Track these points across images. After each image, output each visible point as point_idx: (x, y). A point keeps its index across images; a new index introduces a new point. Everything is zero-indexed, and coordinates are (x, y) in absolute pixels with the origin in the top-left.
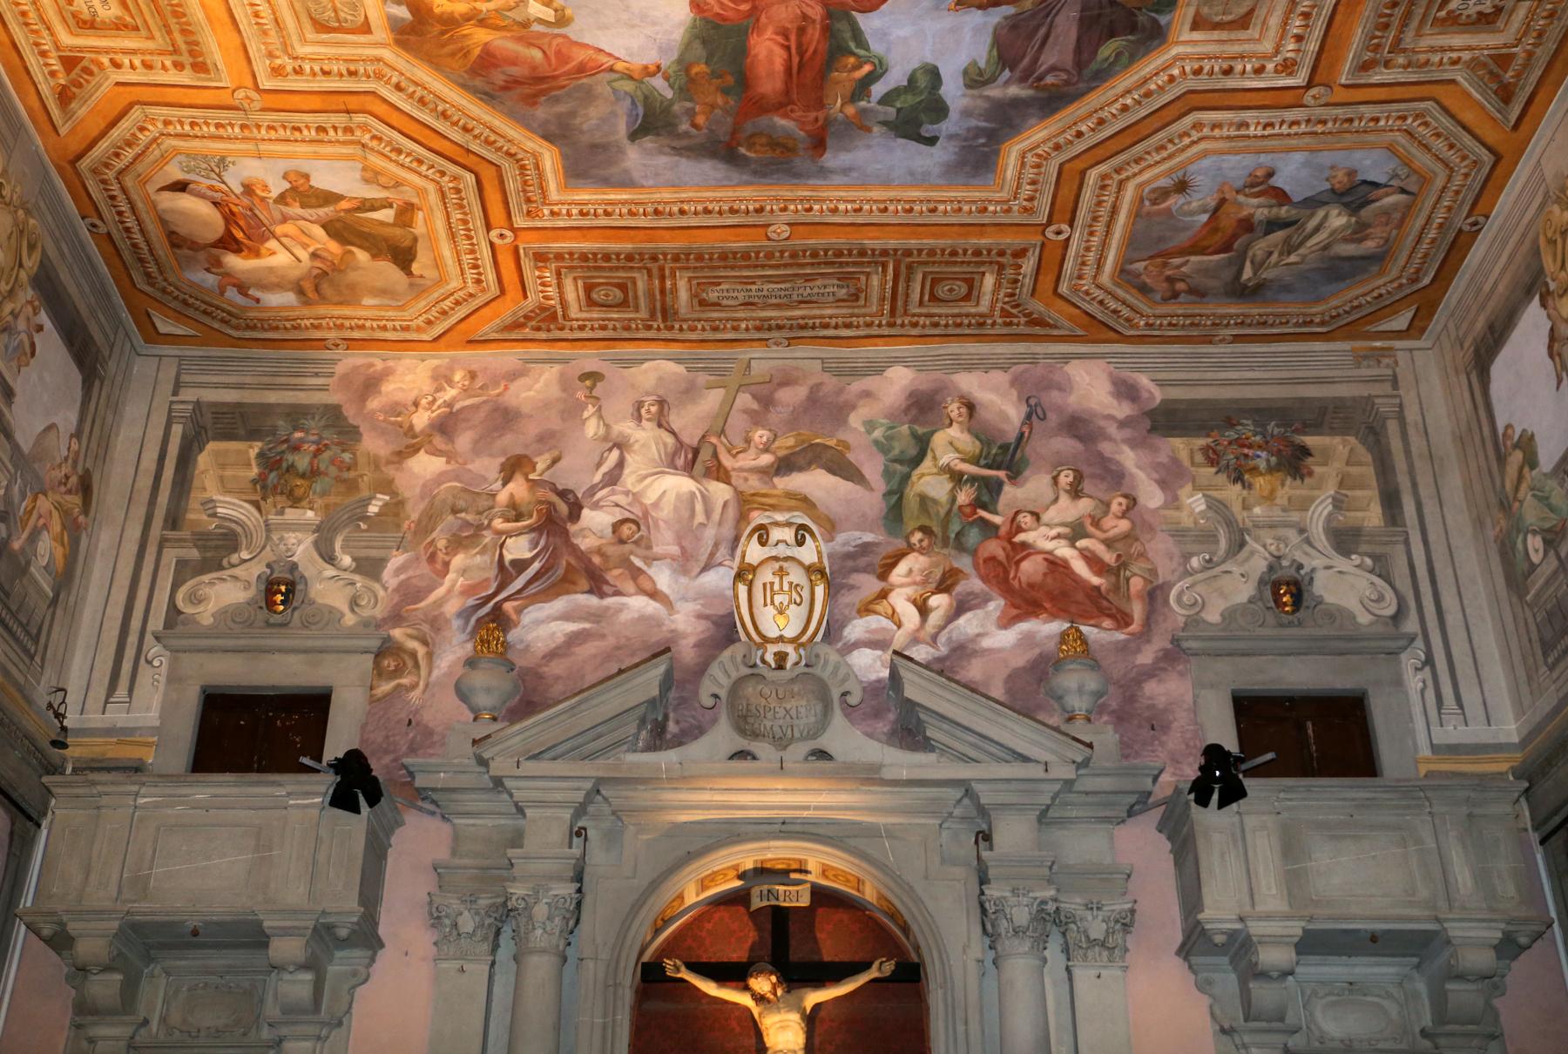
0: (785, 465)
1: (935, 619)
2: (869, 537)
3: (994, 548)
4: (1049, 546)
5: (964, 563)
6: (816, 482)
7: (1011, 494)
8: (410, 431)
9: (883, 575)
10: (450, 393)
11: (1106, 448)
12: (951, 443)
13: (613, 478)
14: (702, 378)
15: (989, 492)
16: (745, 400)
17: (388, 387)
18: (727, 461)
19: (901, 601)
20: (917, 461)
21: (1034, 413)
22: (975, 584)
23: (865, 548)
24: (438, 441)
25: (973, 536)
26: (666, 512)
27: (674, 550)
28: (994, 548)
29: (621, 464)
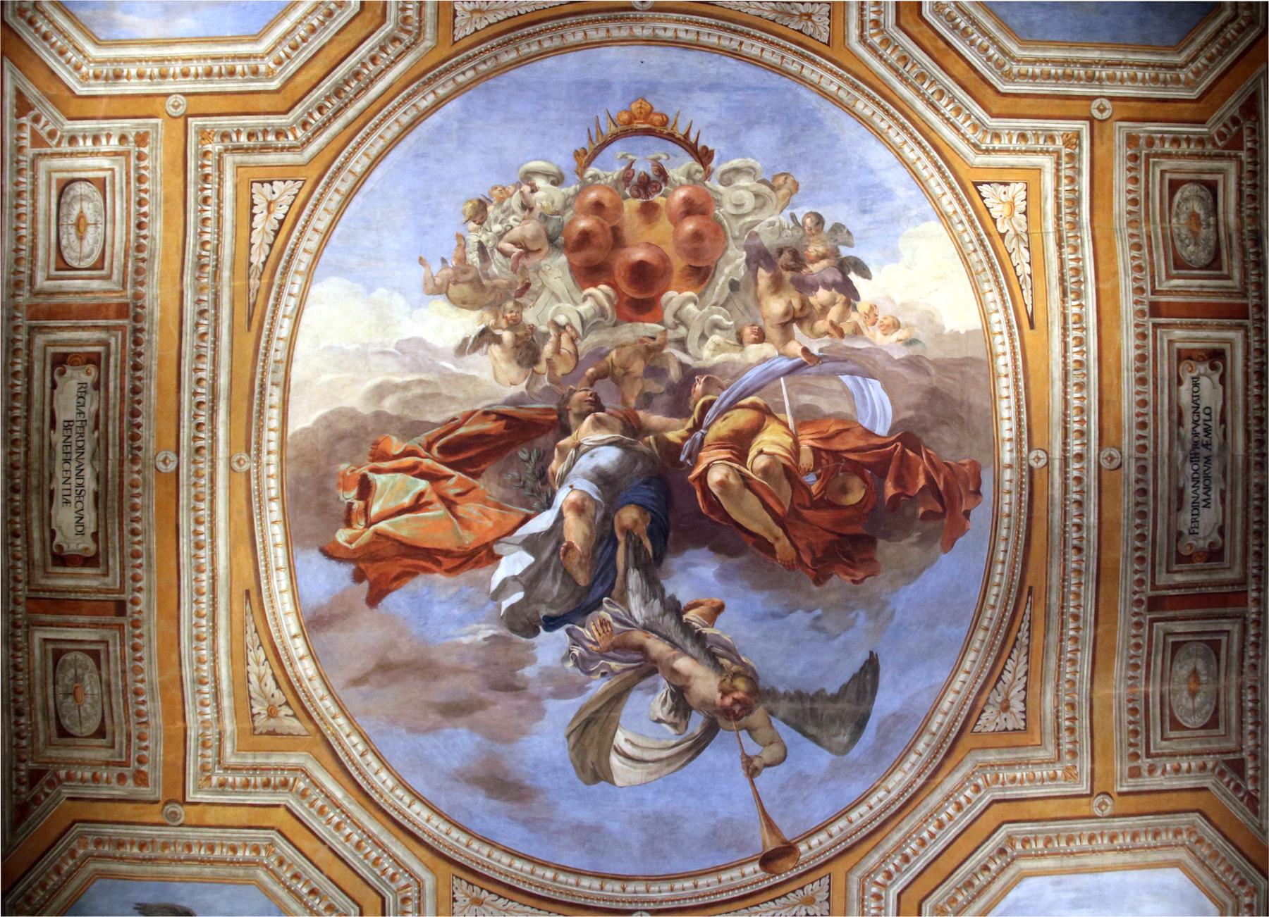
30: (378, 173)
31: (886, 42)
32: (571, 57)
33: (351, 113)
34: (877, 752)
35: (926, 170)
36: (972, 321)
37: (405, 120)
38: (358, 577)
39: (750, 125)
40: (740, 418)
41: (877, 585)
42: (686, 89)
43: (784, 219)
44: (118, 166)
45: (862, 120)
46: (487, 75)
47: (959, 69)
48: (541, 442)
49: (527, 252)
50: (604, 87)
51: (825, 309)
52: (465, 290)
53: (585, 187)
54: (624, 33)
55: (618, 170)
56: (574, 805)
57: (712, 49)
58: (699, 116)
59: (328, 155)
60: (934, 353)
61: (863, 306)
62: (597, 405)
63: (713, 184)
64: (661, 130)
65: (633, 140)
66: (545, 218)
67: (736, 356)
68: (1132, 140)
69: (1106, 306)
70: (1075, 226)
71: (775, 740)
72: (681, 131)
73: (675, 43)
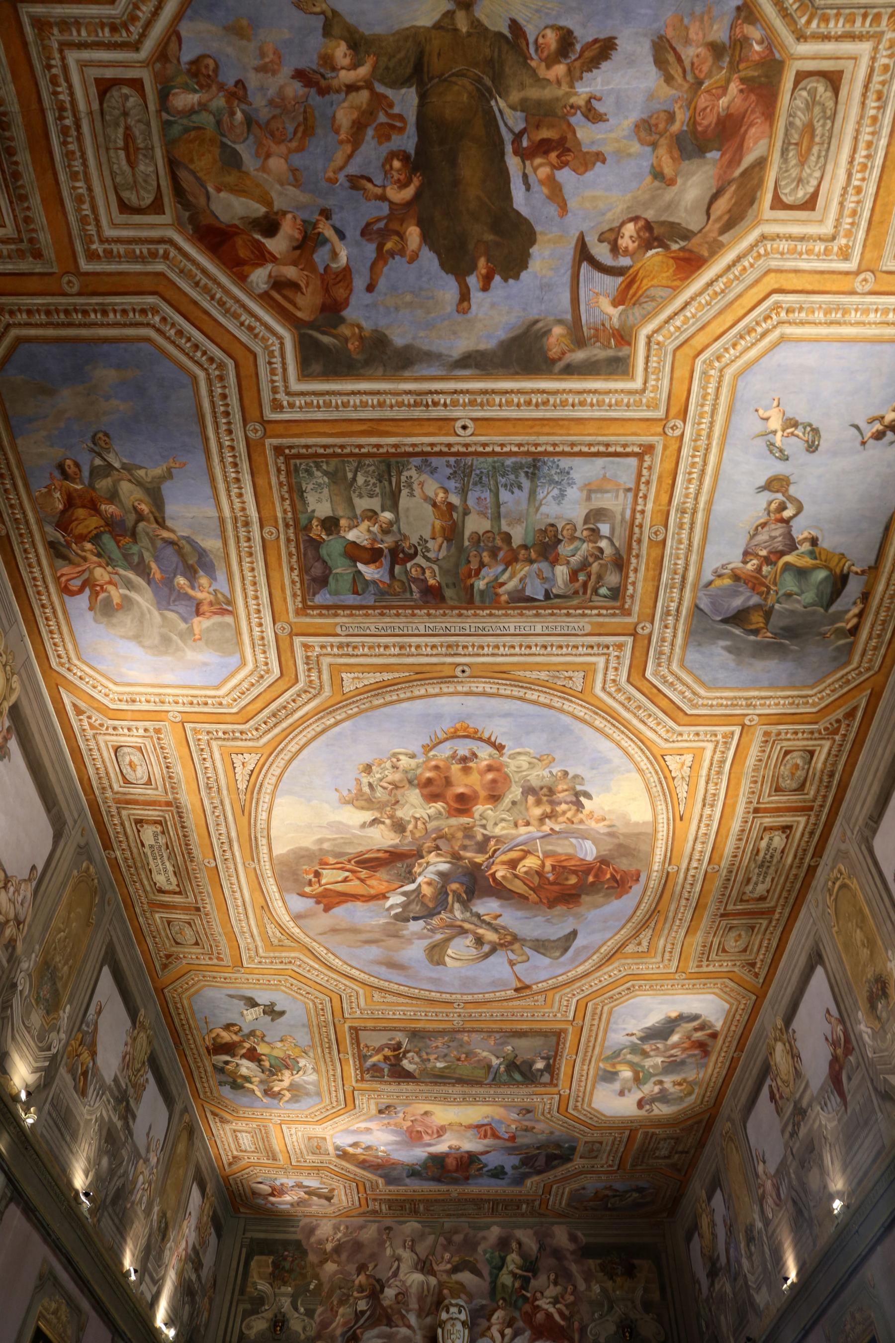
0: (456, 1269)
1: (507, 1339)
2: (484, 1302)
3: (527, 1308)
4: (546, 1307)
5: (517, 1314)
6: (465, 1277)
7: (533, 1283)
8: (325, 1252)
9: (489, 1320)
10: (339, 1235)
11: (566, 1263)
12: (513, 1260)
13: (396, 1274)
14: (427, 1230)
15: (526, 1282)
16: (442, 1240)
17: (318, 1232)
18: (436, 1267)
19: (495, 1331)
20: (500, 1268)
21: (542, 1247)
22: (520, 1324)
23: (483, 1307)
24: (335, 1257)
25: (520, 1301)
26: (413, 1290)
27: (416, 1306)
28: (527, 1308)
29: (398, 1268)
30: (305, 752)
31: (619, 690)
32: (418, 701)
33: (284, 725)
34: (573, 960)
35: (633, 749)
36: (649, 817)
37: (319, 729)
38: (318, 903)
39: (528, 733)
40: (513, 855)
41: (581, 909)
42: (490, 716)
43: (546, 773)
44: (147, 742)
45: (597, 729)
46: (366, 710)
47: (664, 703)
48: (409, 861)
49: (397, 787)
50: (439, 717)
51: (564, 813)
52: (363, 803)
53: (429, 760)
54: (451, 690)
55: (449, 753)
56: (428, 971)
57: (507, 697)
58: (497, 729)
59: (274, 744)
60: (622, 830)
61: (586, 811)
62: (438, 848)
63: (505, 759)
64: (474, 736)
65: (456, 741)
66: (406, 772)
67: (513, 832)
68: (766, 734)
69: (727, 810)
70: (719, 773)
71: (524, 954)
72: (486, 736)
73: (484, 694)
